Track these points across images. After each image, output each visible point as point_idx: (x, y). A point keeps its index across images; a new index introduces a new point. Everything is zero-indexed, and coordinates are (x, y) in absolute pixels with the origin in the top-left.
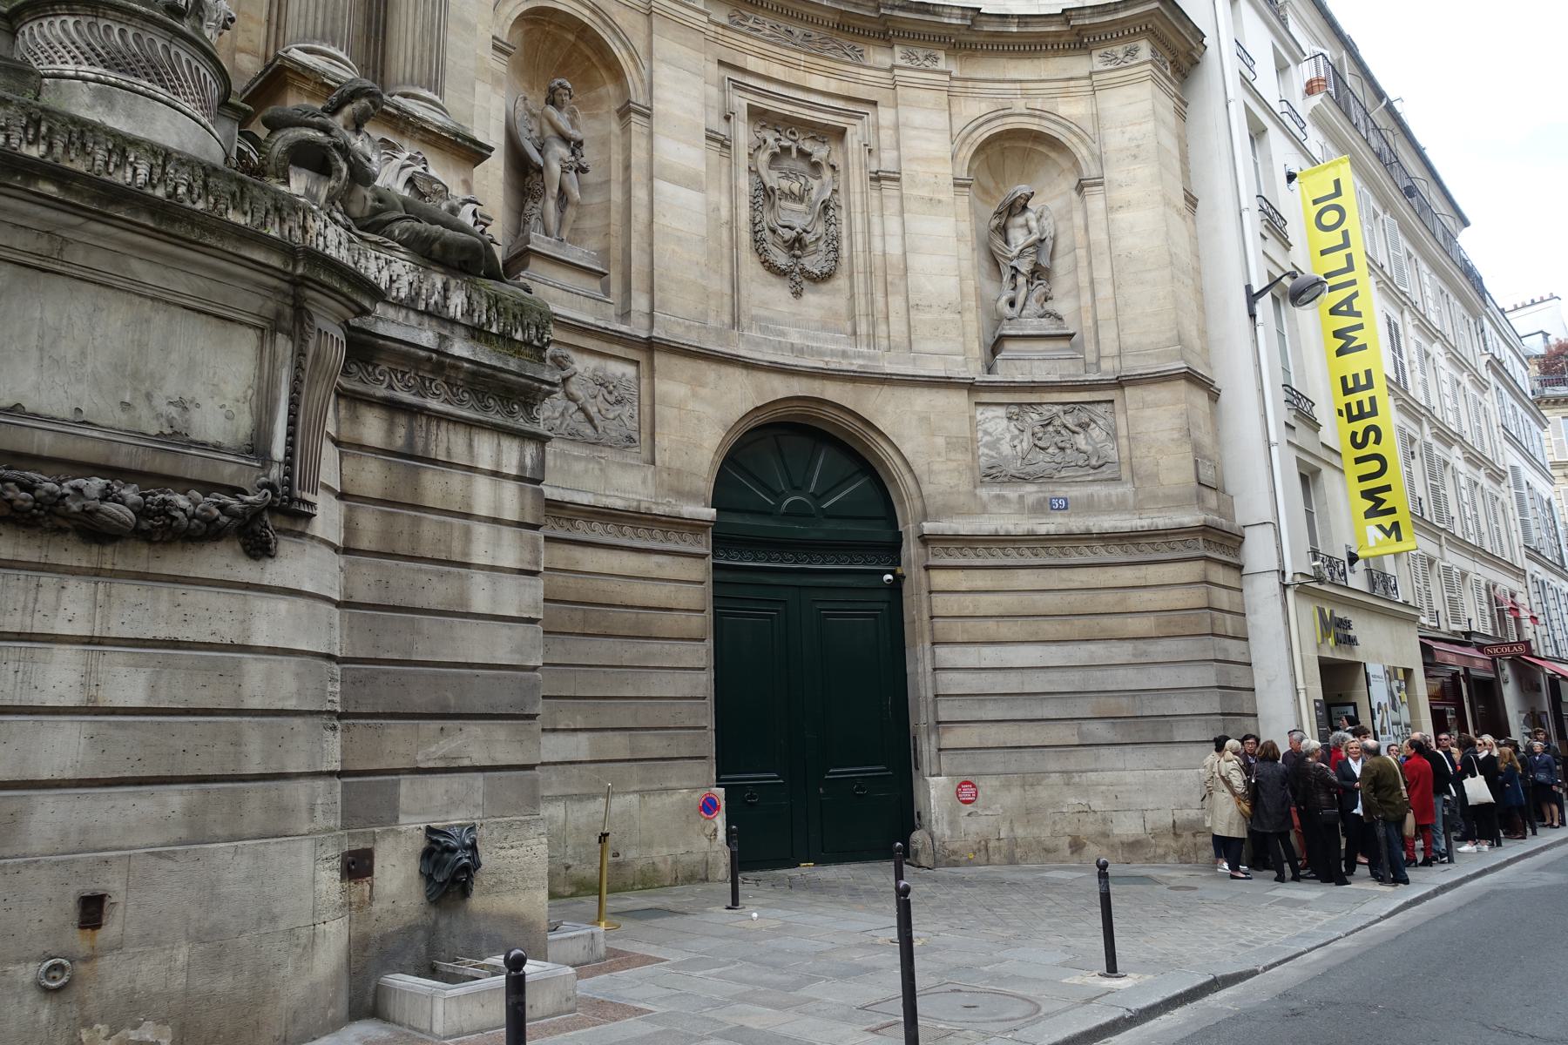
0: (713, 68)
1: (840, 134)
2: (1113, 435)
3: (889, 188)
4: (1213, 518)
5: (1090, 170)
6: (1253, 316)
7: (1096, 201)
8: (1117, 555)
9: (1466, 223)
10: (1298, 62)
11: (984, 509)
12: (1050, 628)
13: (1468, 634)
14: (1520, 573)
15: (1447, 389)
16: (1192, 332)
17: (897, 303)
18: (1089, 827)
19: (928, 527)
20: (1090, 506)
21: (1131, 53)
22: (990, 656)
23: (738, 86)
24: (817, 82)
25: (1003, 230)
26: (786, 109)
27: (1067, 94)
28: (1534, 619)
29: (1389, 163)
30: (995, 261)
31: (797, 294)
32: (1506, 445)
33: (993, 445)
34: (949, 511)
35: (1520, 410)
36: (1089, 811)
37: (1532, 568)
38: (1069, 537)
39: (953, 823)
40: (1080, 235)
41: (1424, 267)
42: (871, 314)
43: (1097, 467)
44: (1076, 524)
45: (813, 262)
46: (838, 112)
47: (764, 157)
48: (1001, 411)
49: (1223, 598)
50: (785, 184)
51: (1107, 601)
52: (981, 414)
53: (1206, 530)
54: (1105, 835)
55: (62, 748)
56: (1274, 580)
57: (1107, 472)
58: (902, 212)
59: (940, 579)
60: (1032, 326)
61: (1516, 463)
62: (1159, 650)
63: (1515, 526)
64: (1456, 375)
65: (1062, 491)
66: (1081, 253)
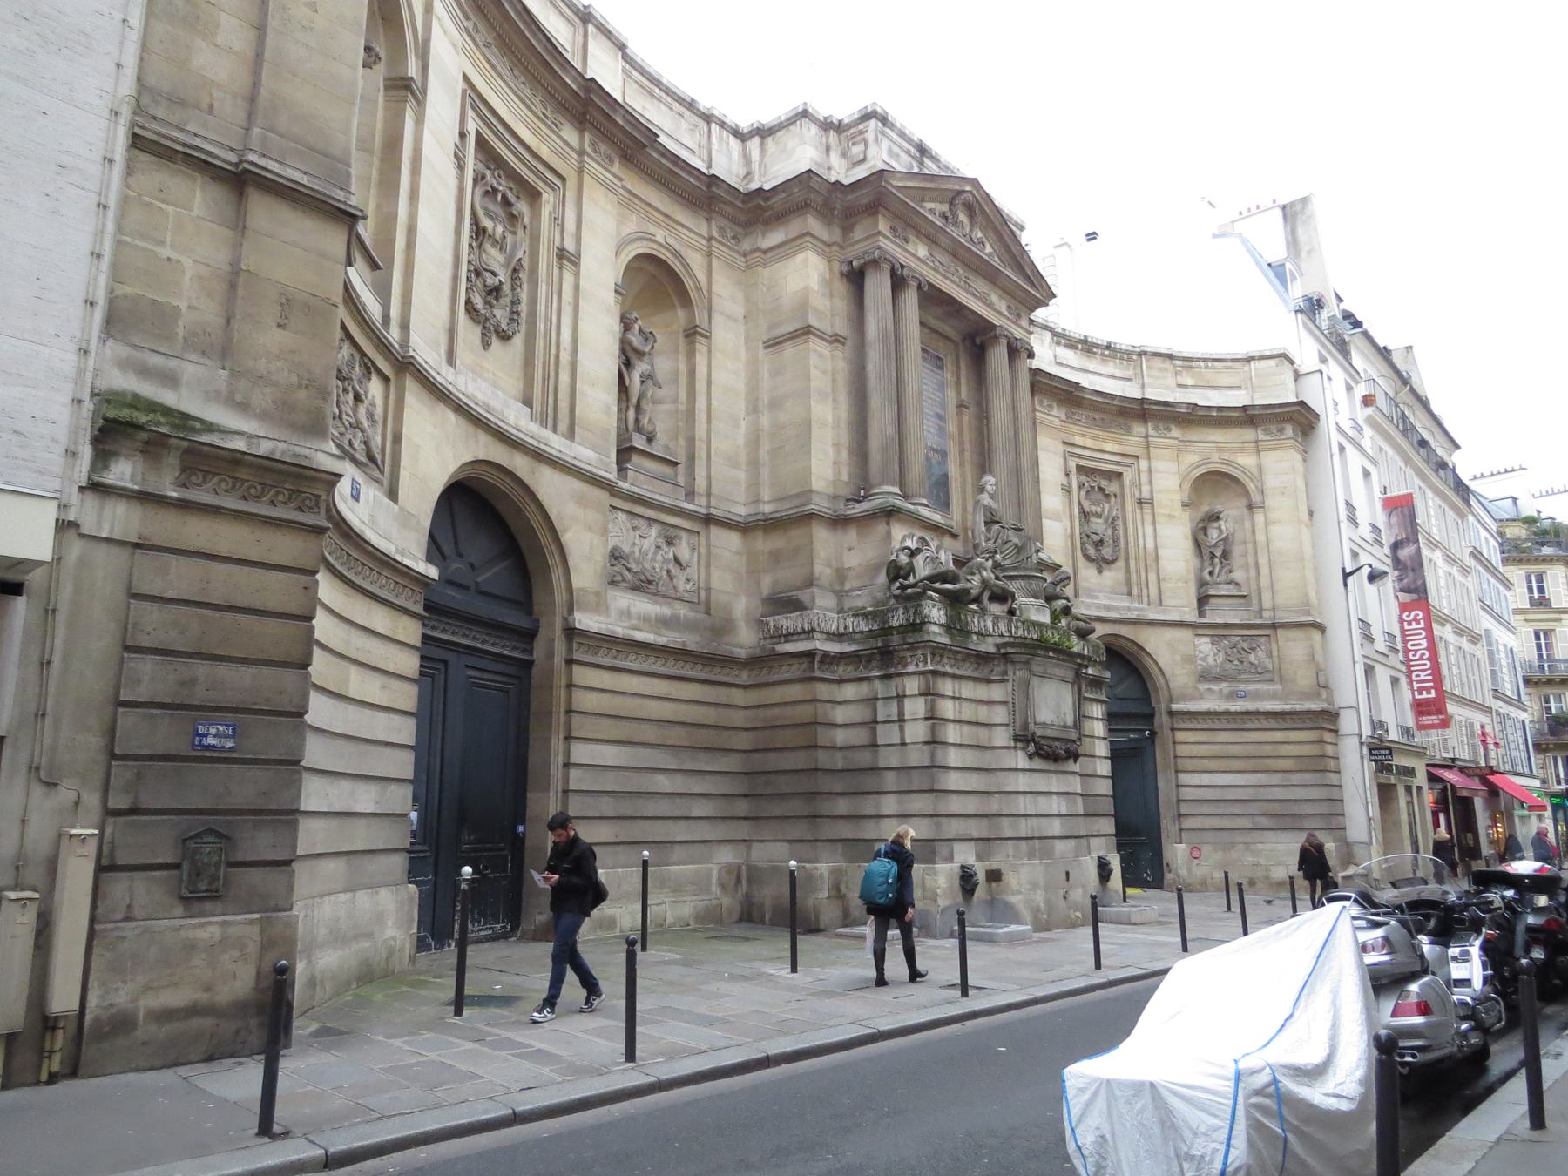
0: (1061, 448)
1: (1120, 475)
2: (1270, 655)
3: (1147, 509)
4: (1325, 706)
5: (1256, 498)
6: (1346, 585)
7: (1259, 518)
8: (1273, 724)
9: (1458, 447)
10: (1357, 383)
11: (1202, 697)
12: (1236, 764)
13: (1453, 760)
14: (1488, 710)
15: (1442, 583)
16: (1312, 595)
17: (1152, 577)
18: (1259, 873)
19: (1175, 707)
20: (1257, 696)
21: (1281, 431)
22: (1206, 779)
23: (1073, 455)
24: (1108, 447)
25: (1205, 529)
26: (1093, 464)
27: (1242, 451)
28: (1496, 744)
29: (1407, 429)
30: (1198, 546)
31: (1100, 572)
32: (1482, 613)
33: (1204, 659)
34: (1184, 698)
35: (1492, 580)
36: (1257, 865)
37: (1497, 705)
38: (1247, 713)
39: (1189, 870)
40: (1249, 534)
41: (1430, 494)
42: (1139, 584)
43: (1259, 672)
44: (1251, 706)
45: (1107, 552)
46: (1118, 463)
47: (1083, 493)
48: (1208, 640)
49: (1330, 750)
50: (1093, 508)
51: (1267, 750)
52: (1198, 641)
53: (1323, 712)
54: (1267, 878)
55: (1056, 827)
56: (1356, 740)
57: (1268, 676)
58: (1154, 523)
59: (1180, 736)
60: (1224, 589)
61: (1490, 626)
62: (1296, 778)
63: (1487, 675)
64: (1448, 568)
65: (1243, 687)
66: (1250, 546)
